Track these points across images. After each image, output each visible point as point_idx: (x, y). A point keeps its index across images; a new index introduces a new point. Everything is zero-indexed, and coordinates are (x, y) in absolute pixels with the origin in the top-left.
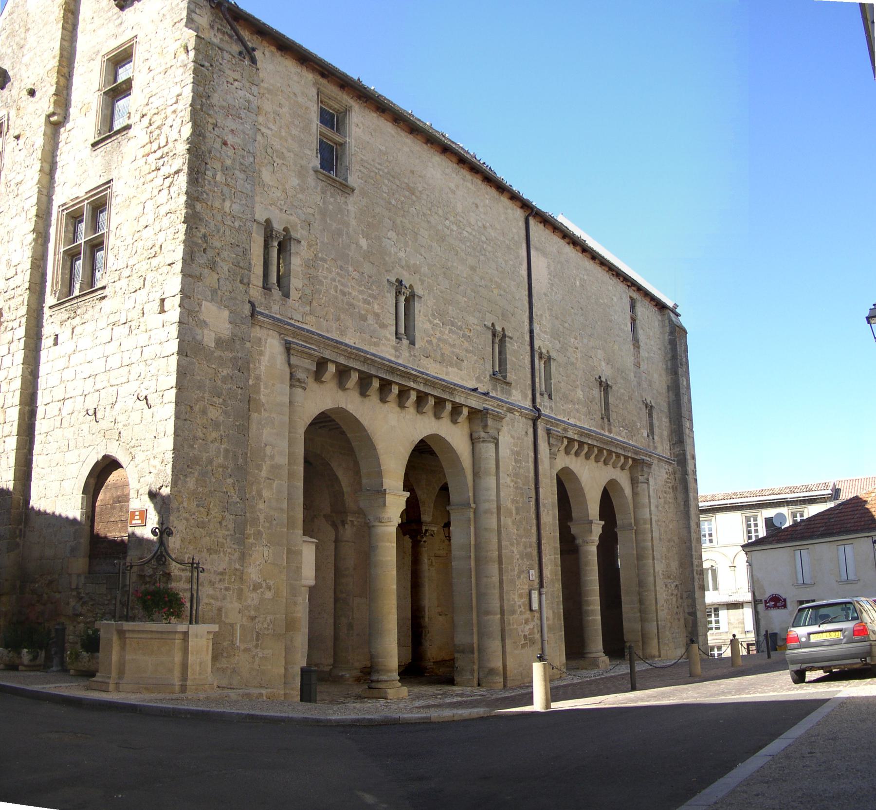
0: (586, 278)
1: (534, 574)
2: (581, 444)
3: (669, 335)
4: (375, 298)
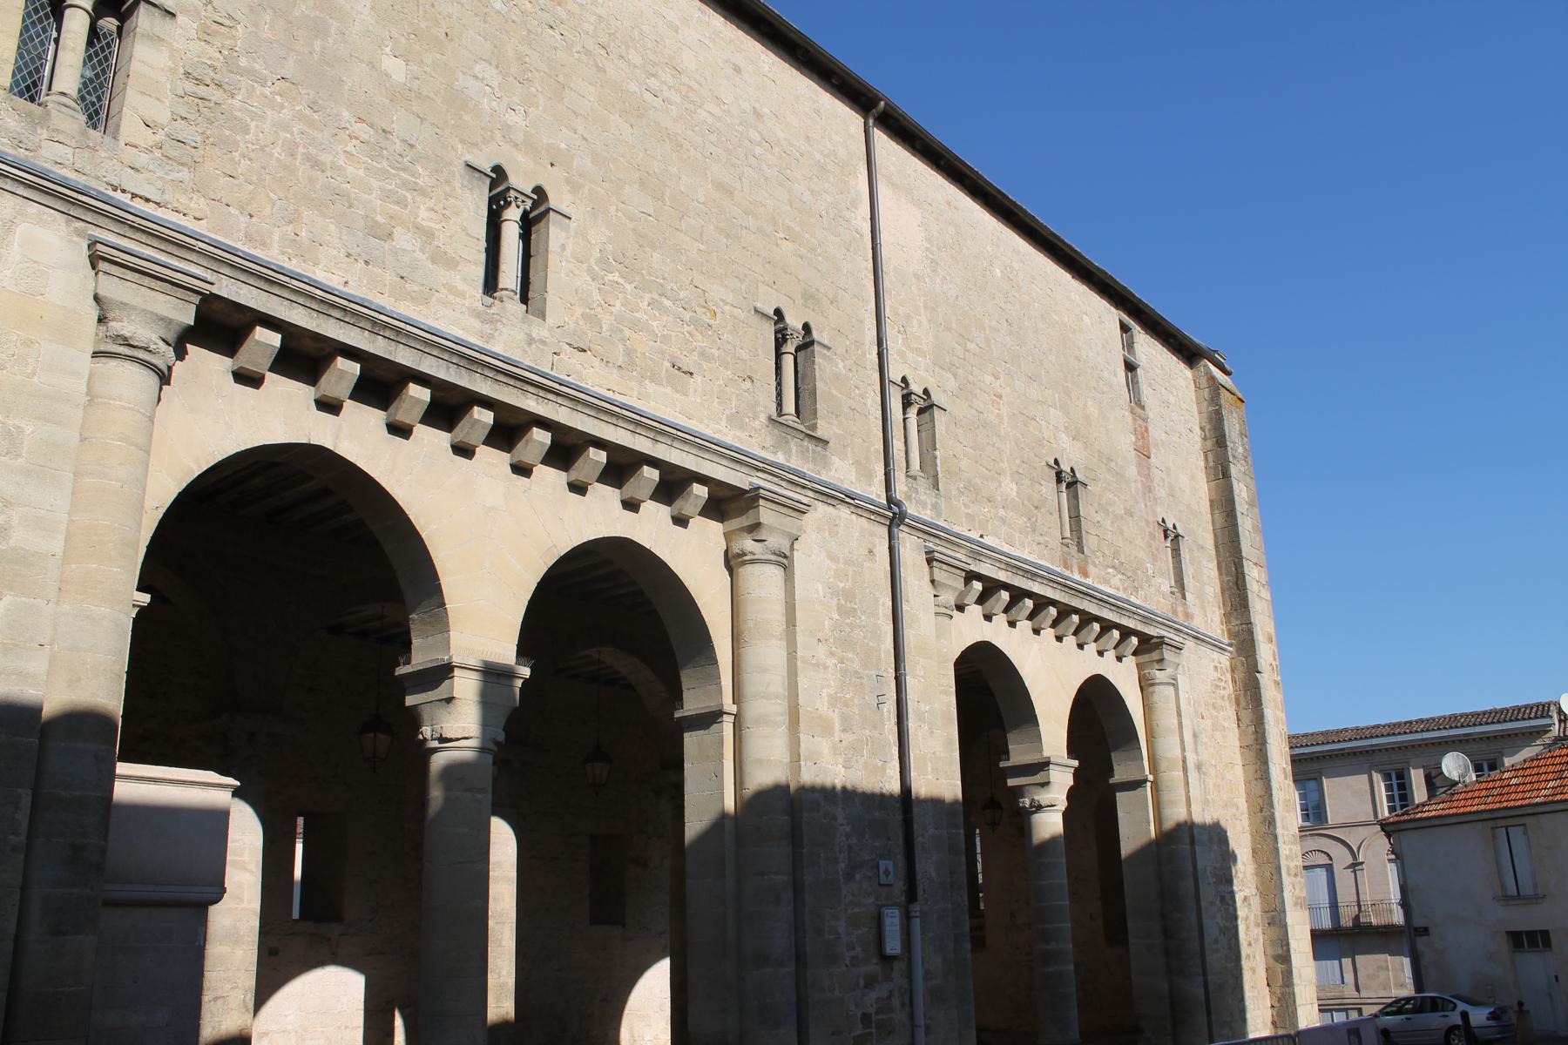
0: (1016, 265)
1: (891, 868)
2: (1018, 595)
3: (1209, 405)
4: (423, 192)
